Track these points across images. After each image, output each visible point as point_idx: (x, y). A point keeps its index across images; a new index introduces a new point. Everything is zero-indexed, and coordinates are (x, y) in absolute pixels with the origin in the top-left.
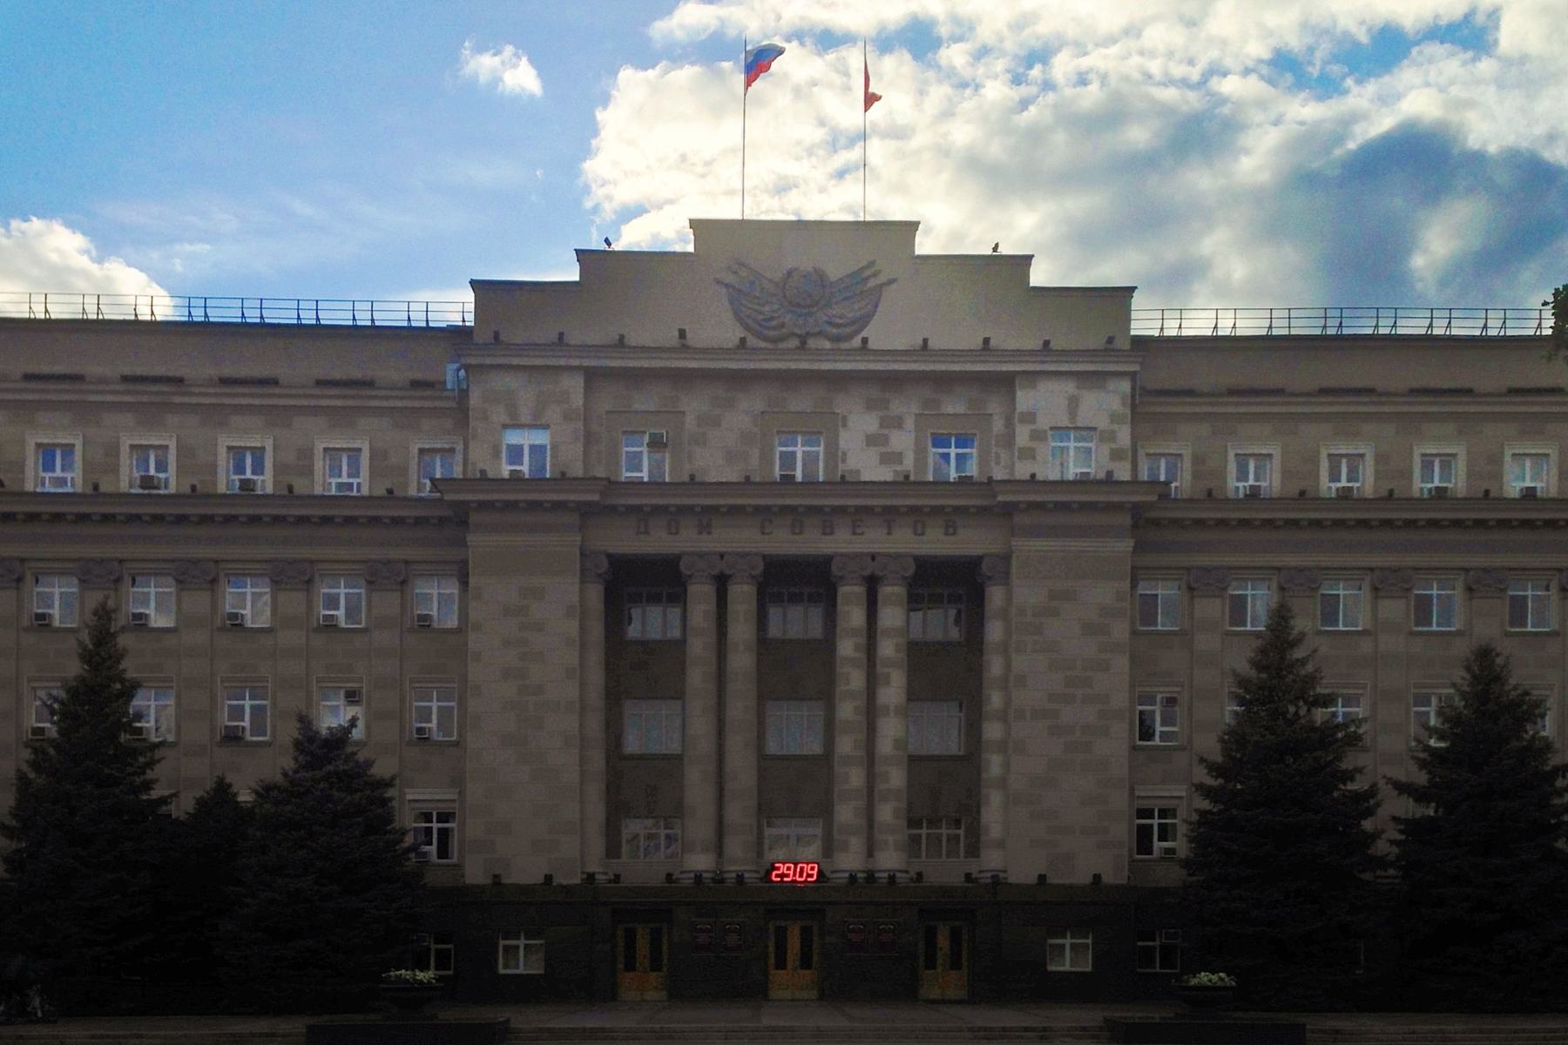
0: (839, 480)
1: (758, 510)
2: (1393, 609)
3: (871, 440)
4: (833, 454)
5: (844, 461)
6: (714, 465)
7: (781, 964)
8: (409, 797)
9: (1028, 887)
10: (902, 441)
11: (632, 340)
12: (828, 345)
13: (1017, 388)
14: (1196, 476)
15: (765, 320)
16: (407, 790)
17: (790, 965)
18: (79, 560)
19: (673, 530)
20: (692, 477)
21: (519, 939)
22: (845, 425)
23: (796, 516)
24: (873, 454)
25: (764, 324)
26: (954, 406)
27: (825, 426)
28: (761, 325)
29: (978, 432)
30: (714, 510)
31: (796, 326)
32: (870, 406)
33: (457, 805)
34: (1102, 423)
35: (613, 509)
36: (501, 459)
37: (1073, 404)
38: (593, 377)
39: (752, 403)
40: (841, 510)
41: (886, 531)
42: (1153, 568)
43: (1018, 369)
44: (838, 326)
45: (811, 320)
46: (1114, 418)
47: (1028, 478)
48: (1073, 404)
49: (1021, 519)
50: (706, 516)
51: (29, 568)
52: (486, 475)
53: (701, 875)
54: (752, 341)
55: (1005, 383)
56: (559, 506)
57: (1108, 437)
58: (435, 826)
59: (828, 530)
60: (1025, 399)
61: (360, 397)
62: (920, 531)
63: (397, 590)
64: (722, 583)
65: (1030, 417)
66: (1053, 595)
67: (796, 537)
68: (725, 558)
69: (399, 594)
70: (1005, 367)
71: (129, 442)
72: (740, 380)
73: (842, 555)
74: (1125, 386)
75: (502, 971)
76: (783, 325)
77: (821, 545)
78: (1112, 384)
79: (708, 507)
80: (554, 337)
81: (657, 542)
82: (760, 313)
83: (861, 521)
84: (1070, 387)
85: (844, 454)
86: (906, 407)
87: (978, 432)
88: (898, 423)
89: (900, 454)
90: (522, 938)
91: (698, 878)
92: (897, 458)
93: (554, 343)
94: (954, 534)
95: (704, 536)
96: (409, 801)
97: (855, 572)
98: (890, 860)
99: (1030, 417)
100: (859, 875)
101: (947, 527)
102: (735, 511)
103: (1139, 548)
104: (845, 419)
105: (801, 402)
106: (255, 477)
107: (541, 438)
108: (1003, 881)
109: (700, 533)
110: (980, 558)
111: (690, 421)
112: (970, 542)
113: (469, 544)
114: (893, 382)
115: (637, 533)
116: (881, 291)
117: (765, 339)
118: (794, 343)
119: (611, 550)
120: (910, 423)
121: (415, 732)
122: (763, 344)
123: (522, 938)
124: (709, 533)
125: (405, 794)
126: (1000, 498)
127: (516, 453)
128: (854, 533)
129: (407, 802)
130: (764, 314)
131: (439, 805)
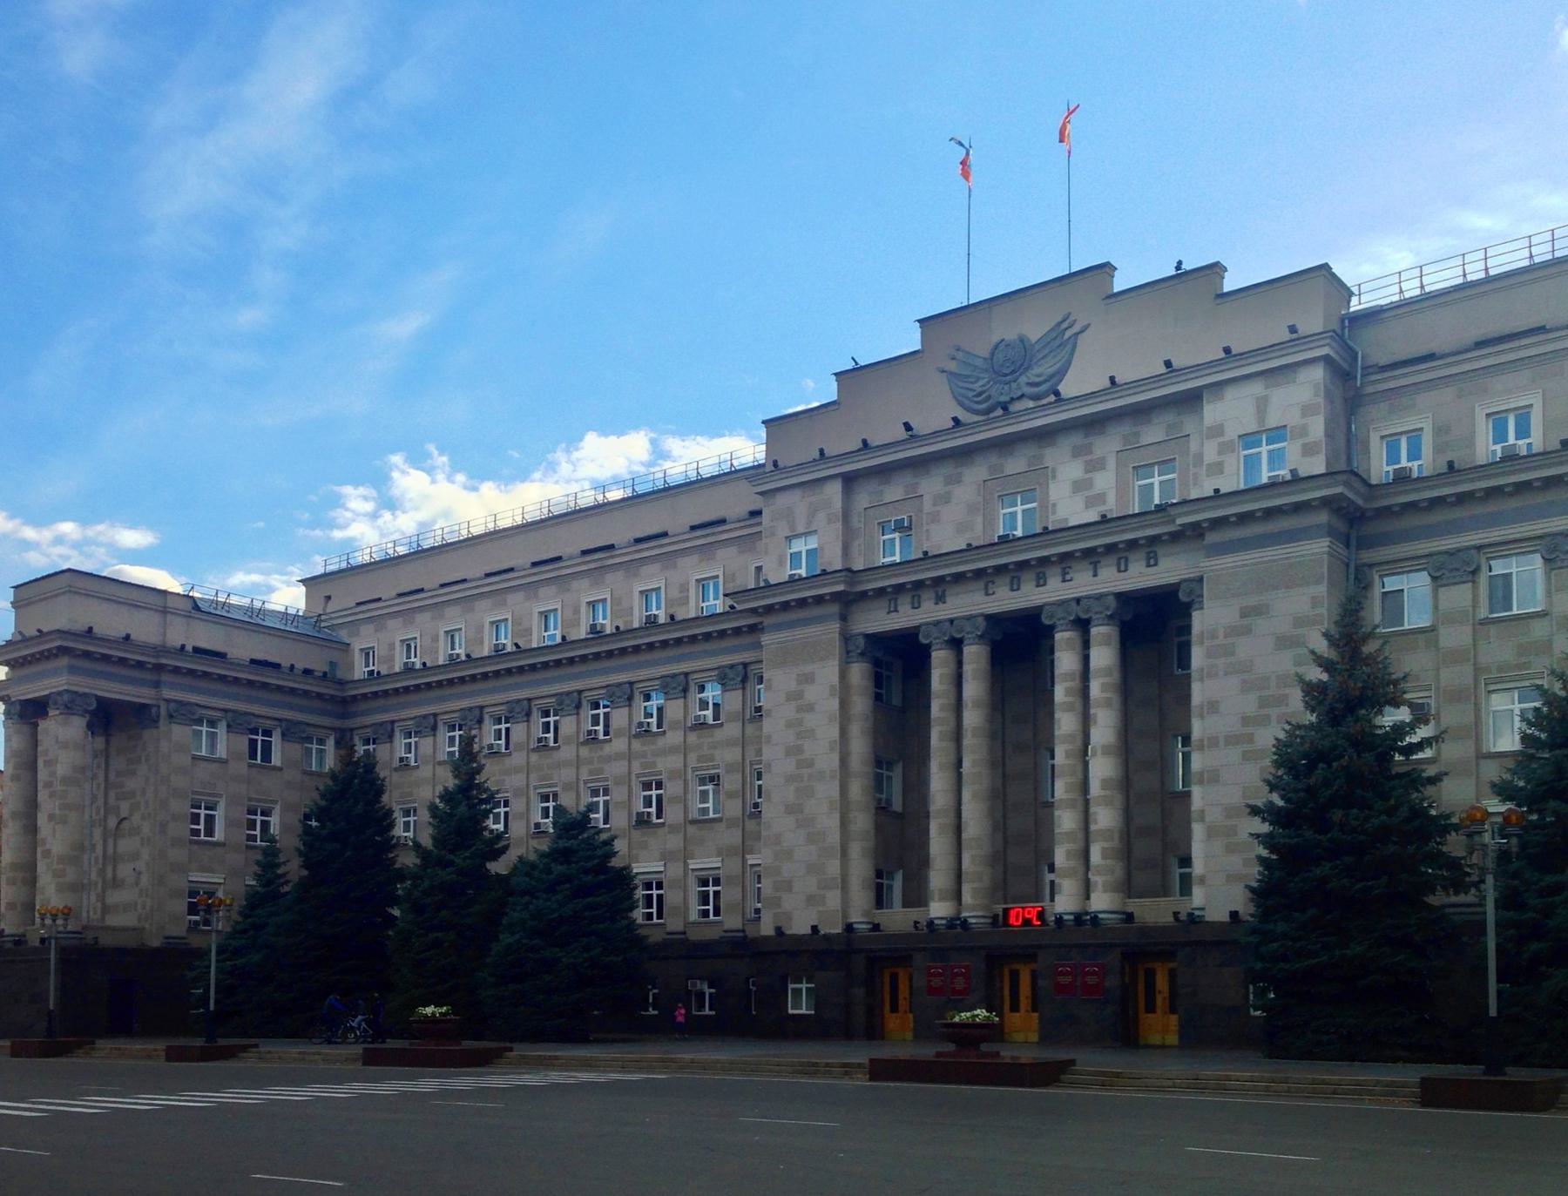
0: (996, 540)
1: (979, 574)
2: (1458, 596)
3: (1078, 486)
4: (1046, 506)
5: (1054, 513)
6: (945, 536)
7: (1151, 1008)
8: (750, 862)
9: (1164, 929)
10: (1105, 481)
11: (875, 441)
12: (1031, 404)
13: (1204, 402)
14: (1438, 449)
15: (976, 396)
16: (748, 857)
17: (1159, 1010)
18: (415, 718)
19: (916, 605)
20: (926, 553)
21: (802, 983)
22: (1054, 477)
23: (1014, 572)
24: (1079, 502)
25: (976, 399)
26: (1153, 433)
27: (1033, 485)
28: (972, 401)
29: (1037, 487)
31: (1002, 394)
32: (1077, 453)
33: (663, 876)
34: (1293, 419)
35: (864, 595)
36: (786, 566)
37: (1262, 406)
38: (850, 481)
39: (976, 473)
41: (1091, 573)
42: (1395, 561)
43: (1237, 375)
44: (1037, 385)
45: (1014, 385)
46: (1307, 411)
47: (1212, 494)
48: (1262, 406)
51: (357, 734)
52: (769, 582)
53: (1061, 917)
54: (964, 416)
55: (1191, 400)
56: (819, 600)
57: (1303, 431)
58: (711, 889)
59: (1041, 581)
60: (1212, 412)
61: (713, 534)
62: (1123, 568)
63: (625, 706)
66: (1245, 613)
67: (1015, 593)
68: (955, 622)
69: (740, 692)
70: (1190, 385)
72: (965, 454)
73: (927, 624)
74: (1318, 373)
75: (694, 1013)
76: (989, 397)
77: (1034, 598)
79: (1064, 553)
80: (817, 455)
81: (903, 618)
82: (971, 390)
83: (1070, 567)
84: (1256, 388)
85: (1054, 505)
86: (1108, 445)
87: (1176, 456)
88: (1096, 466)
89: (1104, 494)
90: (804, 982)
91: (1059, 920)
92: (1100, 498)
93: (815, 460)
94: (1156, 565)
95: (941, 606)
96: (692, 869)
97: (1101, 613)
98: (1102, 902)
99: (1217, 431)
100: (1066, 917)
101: (1148, 559)
102: (959, 578)
104: (1054, 471)
107: (813, 543)
108: (1198, 920)
109: (937, 604)
110: (918, 628)
111: (927, 505)
112: (1169, 570)
113: (763, 643)
114: (1094, 424)
115: (888, 613)
116: (1076, 339)
117: (977, 412)
118: (999, 412)
119: (870, 630)
120: (1112, 463)
121: (533, 826)
122: (977, 418)
123: (804, 982)
124: (944, 603)
125: (688, 865)
126: (1179, 521)
127: (796, 557)
128: (1064, 581)
129: (748, 867)
130: (975, 391)
131: (714, 872)
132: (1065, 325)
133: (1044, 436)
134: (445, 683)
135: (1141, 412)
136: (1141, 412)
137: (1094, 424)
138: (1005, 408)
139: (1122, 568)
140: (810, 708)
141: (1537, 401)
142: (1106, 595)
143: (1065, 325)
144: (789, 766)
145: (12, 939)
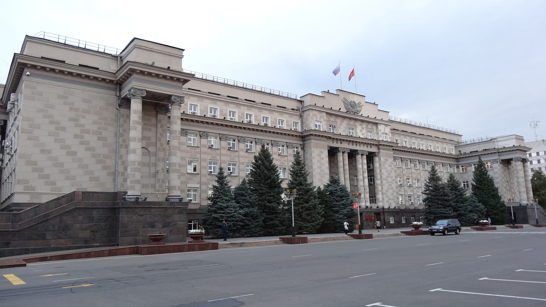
30: (343, 140)
32: (361, 125)
40: (362, 143)
44: (358, 111)
46: (389, 132)
49: (381, 147)
50: (342, 141)
64: (352, 155)
65: (380, 130)
71: (189, 103)
72: (344, 117)
78: (389, 126)
86: (364, 125)
88: (363, 128)
103: (394, 154)
105: (352, 123)
106: (233, 118)
112: (374, 149)
114: (363, 121)
132: (360, 103)
133: (356, 120)
134: (283, 134)
135: (368, 122)
136: (368, 122)
137: (363, 121)
138: (354, 113)
139: (365, 147)
140: (322, 159)
141: (237, 112)
142: (367, 151)
143: (360, 103)
144: (319, 170)
145: (135, 197)
